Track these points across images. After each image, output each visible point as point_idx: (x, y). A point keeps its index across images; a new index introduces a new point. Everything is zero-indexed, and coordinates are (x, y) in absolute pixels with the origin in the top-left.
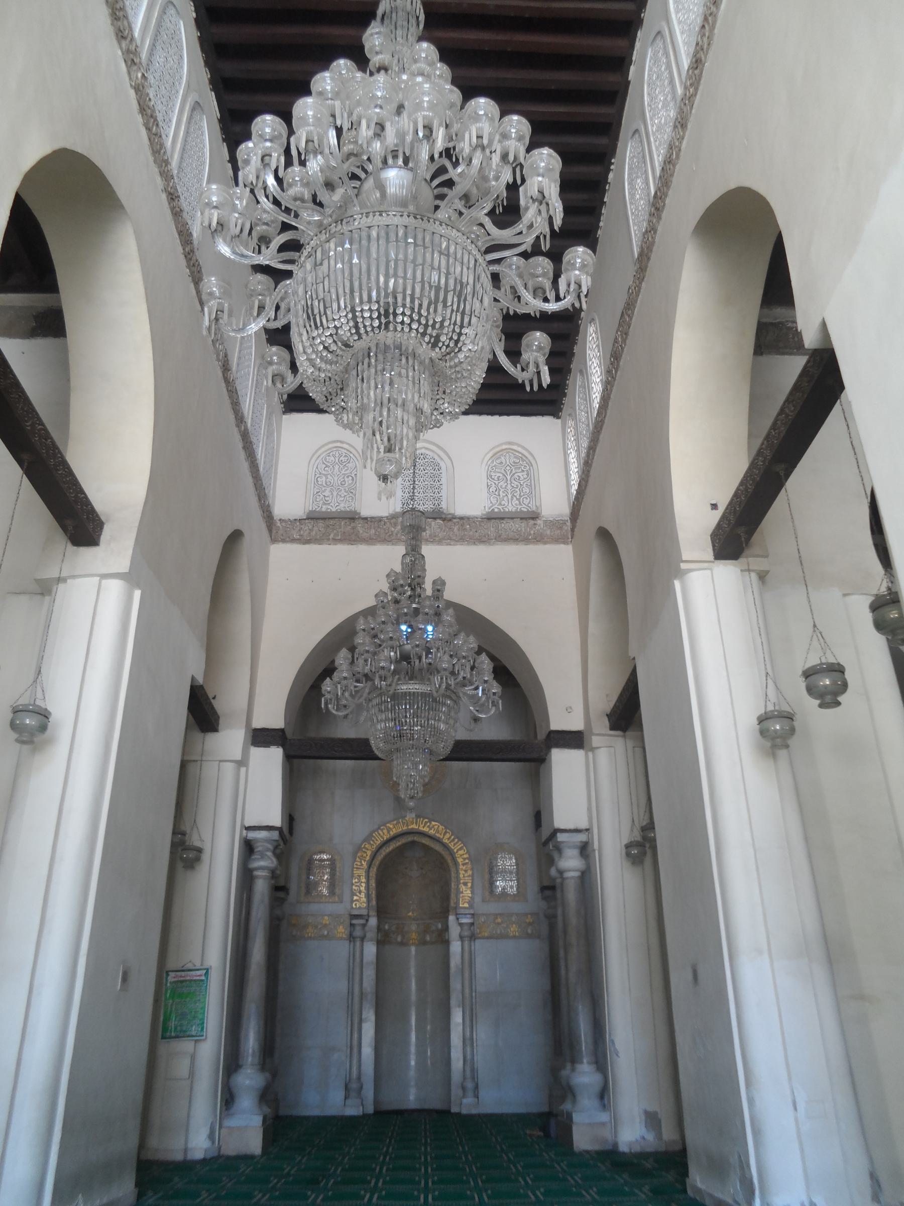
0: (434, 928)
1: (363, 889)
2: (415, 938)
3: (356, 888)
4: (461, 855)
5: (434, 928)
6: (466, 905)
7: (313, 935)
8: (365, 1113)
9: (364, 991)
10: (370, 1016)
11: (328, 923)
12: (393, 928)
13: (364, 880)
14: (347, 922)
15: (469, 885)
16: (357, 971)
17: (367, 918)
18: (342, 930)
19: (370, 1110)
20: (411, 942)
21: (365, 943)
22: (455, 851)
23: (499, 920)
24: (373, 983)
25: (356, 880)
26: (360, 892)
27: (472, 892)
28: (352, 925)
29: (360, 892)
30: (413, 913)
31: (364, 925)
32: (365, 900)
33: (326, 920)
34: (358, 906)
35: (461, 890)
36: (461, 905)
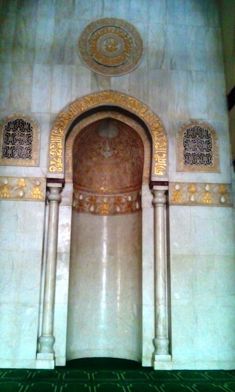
1: (59, 154)
2: (107, 208)
3: (53, 154)
4: (156, 129)
5: (124, 200)
6: (161, 173)
7: (8, 196)
8: (57, 365)
9: (58, 251)
10: (63, 271)
11: (24, 184)
12: (87, 199)
13: (61, 147)
14: (44, 185)
15: (164, 155)
16: (52, 231)
17: (62, 182)
18: (40, 192)
19: (62, 362)
20: (103, 212)
21: (61, 207)
22: (151, 124)
23: (193, 189)
24: (68, 243)
25: (53, 147)
26: (57, 157)
27: (167, 162)
28: (48, 189)
29: (57, 157)
30: (105, 188)
31: (61, 190)
32: (62, 165)
33: (22, 182)
34: (54, 170)
35: (156, 160)
36: (156, 174)
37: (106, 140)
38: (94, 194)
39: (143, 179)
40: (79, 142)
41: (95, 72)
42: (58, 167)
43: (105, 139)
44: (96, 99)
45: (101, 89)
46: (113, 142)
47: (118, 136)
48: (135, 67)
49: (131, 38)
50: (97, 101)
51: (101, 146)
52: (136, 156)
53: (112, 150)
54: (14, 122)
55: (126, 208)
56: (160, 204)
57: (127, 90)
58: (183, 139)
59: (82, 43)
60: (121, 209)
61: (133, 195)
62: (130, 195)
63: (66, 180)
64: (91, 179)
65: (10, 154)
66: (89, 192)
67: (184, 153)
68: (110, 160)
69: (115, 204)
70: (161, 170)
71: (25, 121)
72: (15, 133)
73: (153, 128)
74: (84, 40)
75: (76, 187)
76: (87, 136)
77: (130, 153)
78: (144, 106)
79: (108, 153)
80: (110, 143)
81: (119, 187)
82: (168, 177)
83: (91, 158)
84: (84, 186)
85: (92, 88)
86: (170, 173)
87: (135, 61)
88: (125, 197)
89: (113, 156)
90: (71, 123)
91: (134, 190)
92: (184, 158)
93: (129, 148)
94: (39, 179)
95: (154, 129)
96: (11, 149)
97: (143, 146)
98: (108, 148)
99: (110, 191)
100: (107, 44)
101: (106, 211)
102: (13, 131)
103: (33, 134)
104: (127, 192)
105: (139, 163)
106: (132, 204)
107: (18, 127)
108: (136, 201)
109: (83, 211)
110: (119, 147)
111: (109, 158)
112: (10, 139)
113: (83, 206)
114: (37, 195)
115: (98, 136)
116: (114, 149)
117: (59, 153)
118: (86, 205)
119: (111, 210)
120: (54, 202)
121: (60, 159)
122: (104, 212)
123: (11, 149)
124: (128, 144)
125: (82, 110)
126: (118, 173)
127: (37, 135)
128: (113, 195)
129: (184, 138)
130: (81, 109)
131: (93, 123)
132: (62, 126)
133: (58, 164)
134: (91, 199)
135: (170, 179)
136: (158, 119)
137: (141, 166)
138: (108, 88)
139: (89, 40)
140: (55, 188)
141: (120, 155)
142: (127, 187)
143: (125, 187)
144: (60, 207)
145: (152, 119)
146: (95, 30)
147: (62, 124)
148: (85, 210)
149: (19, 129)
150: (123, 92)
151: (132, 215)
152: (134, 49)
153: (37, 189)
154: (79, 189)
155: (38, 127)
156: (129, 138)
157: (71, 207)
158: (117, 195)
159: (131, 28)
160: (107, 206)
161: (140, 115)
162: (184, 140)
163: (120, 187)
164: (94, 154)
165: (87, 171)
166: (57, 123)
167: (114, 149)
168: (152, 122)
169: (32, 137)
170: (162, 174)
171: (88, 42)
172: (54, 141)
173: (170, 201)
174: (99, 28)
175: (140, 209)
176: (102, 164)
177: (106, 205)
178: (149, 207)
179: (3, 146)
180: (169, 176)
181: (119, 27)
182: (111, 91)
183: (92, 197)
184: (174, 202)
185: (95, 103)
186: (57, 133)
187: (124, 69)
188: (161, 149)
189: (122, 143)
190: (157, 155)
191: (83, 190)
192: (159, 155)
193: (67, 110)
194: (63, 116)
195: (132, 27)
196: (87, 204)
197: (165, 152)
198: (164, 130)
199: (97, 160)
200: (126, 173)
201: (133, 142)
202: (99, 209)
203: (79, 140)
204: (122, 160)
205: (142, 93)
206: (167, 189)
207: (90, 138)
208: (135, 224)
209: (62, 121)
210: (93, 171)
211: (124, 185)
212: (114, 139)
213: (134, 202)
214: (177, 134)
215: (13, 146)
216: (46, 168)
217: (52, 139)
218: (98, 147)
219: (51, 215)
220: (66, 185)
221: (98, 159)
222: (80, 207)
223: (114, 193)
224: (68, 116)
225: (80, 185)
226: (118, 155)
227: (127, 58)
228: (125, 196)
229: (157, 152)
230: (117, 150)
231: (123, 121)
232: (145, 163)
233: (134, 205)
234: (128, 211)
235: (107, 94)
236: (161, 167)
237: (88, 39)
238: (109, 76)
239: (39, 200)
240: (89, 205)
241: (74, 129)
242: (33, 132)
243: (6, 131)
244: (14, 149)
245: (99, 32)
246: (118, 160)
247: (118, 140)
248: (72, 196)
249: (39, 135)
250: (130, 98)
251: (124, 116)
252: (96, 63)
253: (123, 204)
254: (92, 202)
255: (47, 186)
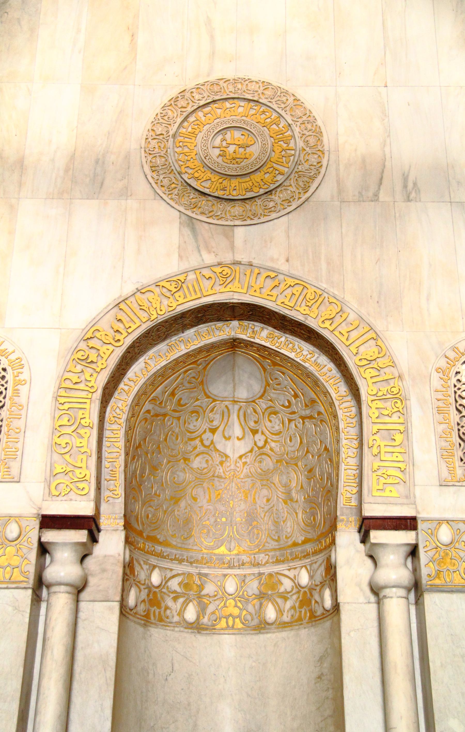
0: (287, 584)
2: (236, 612)
12: (174, 584)
20: (223, 623)
30: (230, 550)
35: (375, 451)
37: (230, 407)
38: (197, 567)
39: (338, 513)
40: (148, 411)
41: (194, 215)
42: (76, 480)
43: (227, 403)
44: (193, 286)
45: (209, 259)
46: (250, 410)
47: (265, 392)
48: (303, 199)
49: (289, 125)
50: (195, 291)
51: (216, 423)
52: (315, 449)
53: (249, 437)
55: (293, 608)
56: (394, 590)
57: (282, 260)
58: (453, 389)
59: (154, 143)
60: (280, 612)
61: (315, 566)
62: (305, 566)
63: (104, 522)
64: (188, 521)
66: (181, 561)
67: (459, 430)
68: (245, 463)
69: (262, 596)
70: (390, 481)
73: (360, 360)
74: (161, 137)
75: (141, 545)
76: (173, 394)
77: (301, 442)
78: (332, 300)
79: (237, 442)
80: (241, 413)
81: (273, 544)
82: (415, 503)
83: (186, 459)
84: (166, 544)
85: (180, 257)
86: (418, 491)
87: (301, 184)
88: (291, 574)
89: (251, 451)
90: (119, 352)
91: (315, 553)
92: (460, 445)
93: (296, 426)
94: (17, 519)
95: (366, 362)
97: (335, 416)
98: (238, 431)
99: (245, 558)
100: (224, 144)
101: (234, 622)
103: (6, 389)
104: (295, 558)
105: (326, 467)
106: (311, 595)
108: (322, 584)
109: (161, 620)
110: (268, 424)
111: (241, 457)
113: (163, 605)
114: (8, 569)
115: (206, 394)
116: (255, 432)
117: (81, 440)
118: (169, 602)
119: (249, 617)
120: (63, 588)
121: (84, 457)
122: (227, 623)
124: (294, 413)
125: (153, 318)
126: (268, 500)
127: (16, 392)
128: (256, 570)
129: (455, 386)
130: (150, 315)
131: (188, 355)
132: (92, 362)
133: (77, 471)
134: (186, 586)
135: (420, 509)
136: (374, 336)
137: (334, 475)
138: (228, 258)
139: (174, 136)
140: (65, 544)
141: (271, 449)
142: (295, 544)
143: (290, 543)
144: (82, 605)
145: (354, 335)
146: (189, 109)
147: (93, 357)
148: (167, 617)
150: (270, 264)
151: (313, 630)
152: (298, 152)
153: (10, 550)
154: (153, 553)
155: (22, 366)
156: (296, 396)
157: (116, 606)
158: (266, 570)
159: (291, 99)
160: (236, 606)
161: (322, 326)
162: (455, 392)
163: (276, 543)
164: (195, 448)
165: (176, 500)
166: (79, 355)
167: (255, 432)
168: (357, 343)
169: (4, 398)
170: (395, 494)
171: (171, 140)
172: (66, 406)
173: (424, 580)
174: (202, 103)
175: (336, 607)
176: (219, 477)
177: (235, 600)
178: (362, 599)
180: (418, 501)
181: (255, 99)
182: (239, 263)
183: (190, 575)
184: (437, 582)
185: (189, 298)
186: (76, 383)
187: (272, 204)
188: (388, 420)
189: (275, 413)
190: (375, 437)
191: (160, 556)
192: (383, 438)
193: (110, 317)
194: (98, 335)
195: (293, 98)
196: (175, 599)
197: (402, 428)
198: (394, 365)
199: (205, 466)
200: (291, 500)
201: (306, 406)
202: (213, 613)
203: (147, 406)
204: (277, 461)
205: (324, 266)
206: (414, 542)
207: (181, 399)
208: (321, 659)
209: (92, 347)
210: (195, 499)
211: (287, 538)
212: (254, 401)
213: (318, 588)
214: (435, 376)
216: (42, 485)
217: (62, 400)
218: (206, 426)
219: (49, 634)
220: (102, 537)
221: (207, 461)
222: (152, 609)
223: (258, 565)
224: (111, 333)
225: (153, 539)
226: (267, 449)
227: (280, 178)
228: (289, 570)
229: (376, 428)
230: (263, 433)
231: (274, 348)
232: (343, 467)
233: (316, 597)
234: (300, 619)
235: (224, 273)
236: (391, 472)
237: (171, 133)
238: (232, 223)
239: (14, 586)
240: (181, 600)
241: (130, 374)
242: (7, 382)
245: (200, 114)
246: (268, 463)
247: (263, 404)
248: (120, 571)
249: (24, 390)
250: (291, 282)
251: (277, 333)
252: (193, 191)
253: (284, 597)
254: (191, 593)
255: (40, 539)
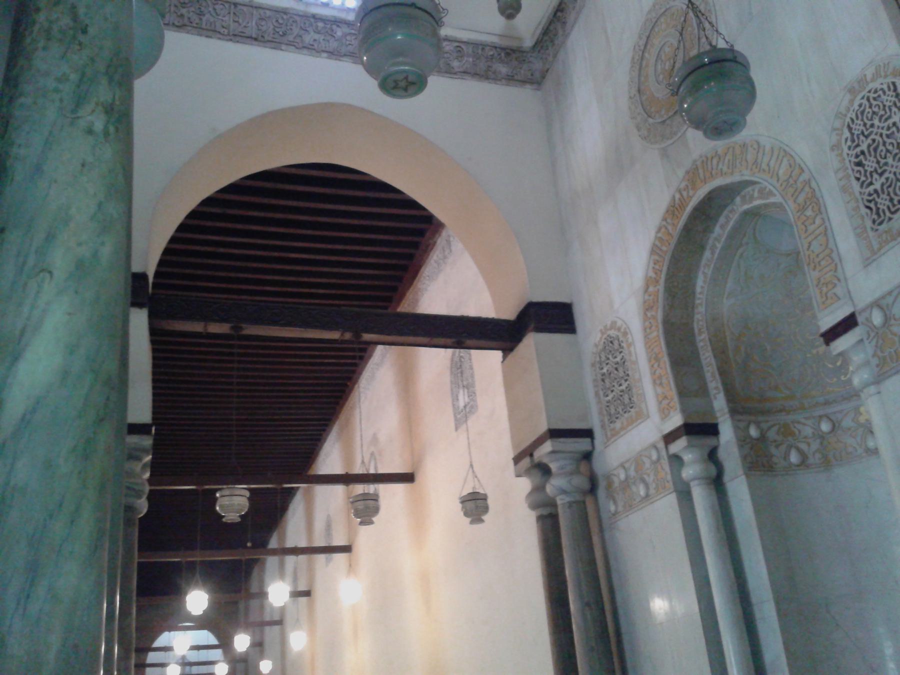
54: (858, 110)
65: (889, 208)
71: (879, 87)
72: (874, 140)
96: (883, 193)
102: (866, 137)
107: (872, 119)
112: (870, 164)
123: (883, 193)
149: (876, 122)
179: (863, 199)
215: (883, 179)
243: (850, 152)
244: (890, 186)
